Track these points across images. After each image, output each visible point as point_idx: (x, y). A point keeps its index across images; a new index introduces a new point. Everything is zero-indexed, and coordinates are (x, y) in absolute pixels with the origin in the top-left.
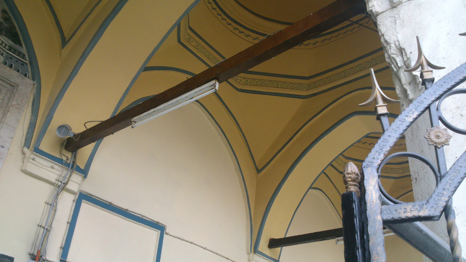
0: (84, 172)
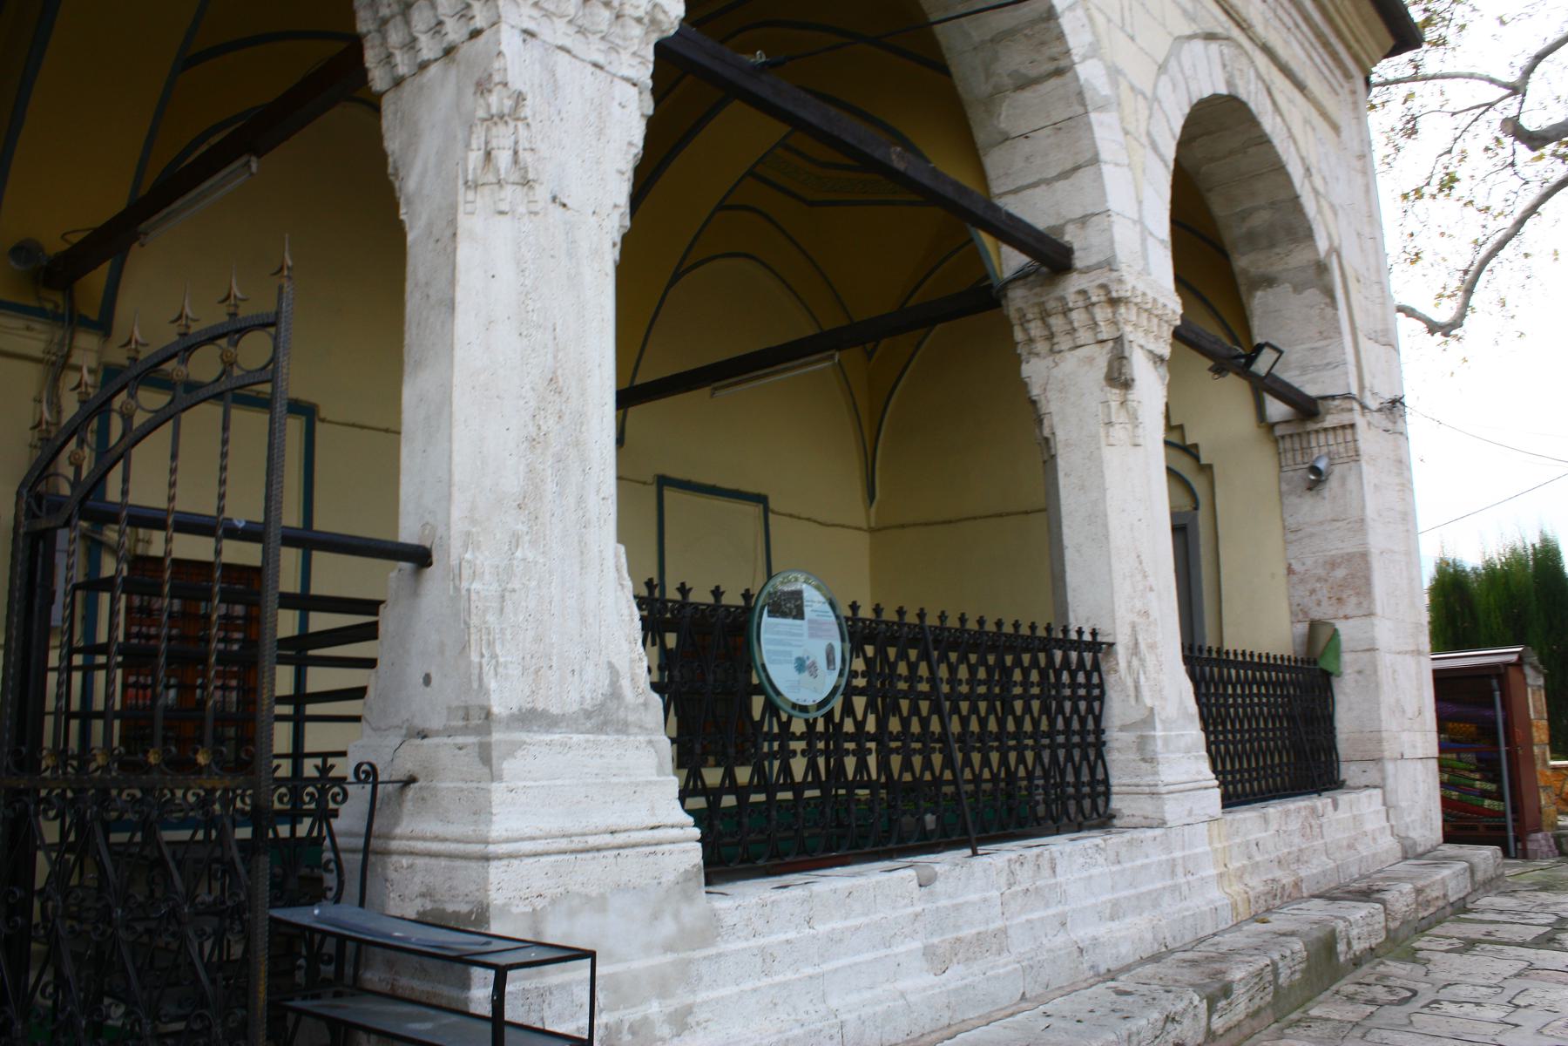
0: (104, 325)
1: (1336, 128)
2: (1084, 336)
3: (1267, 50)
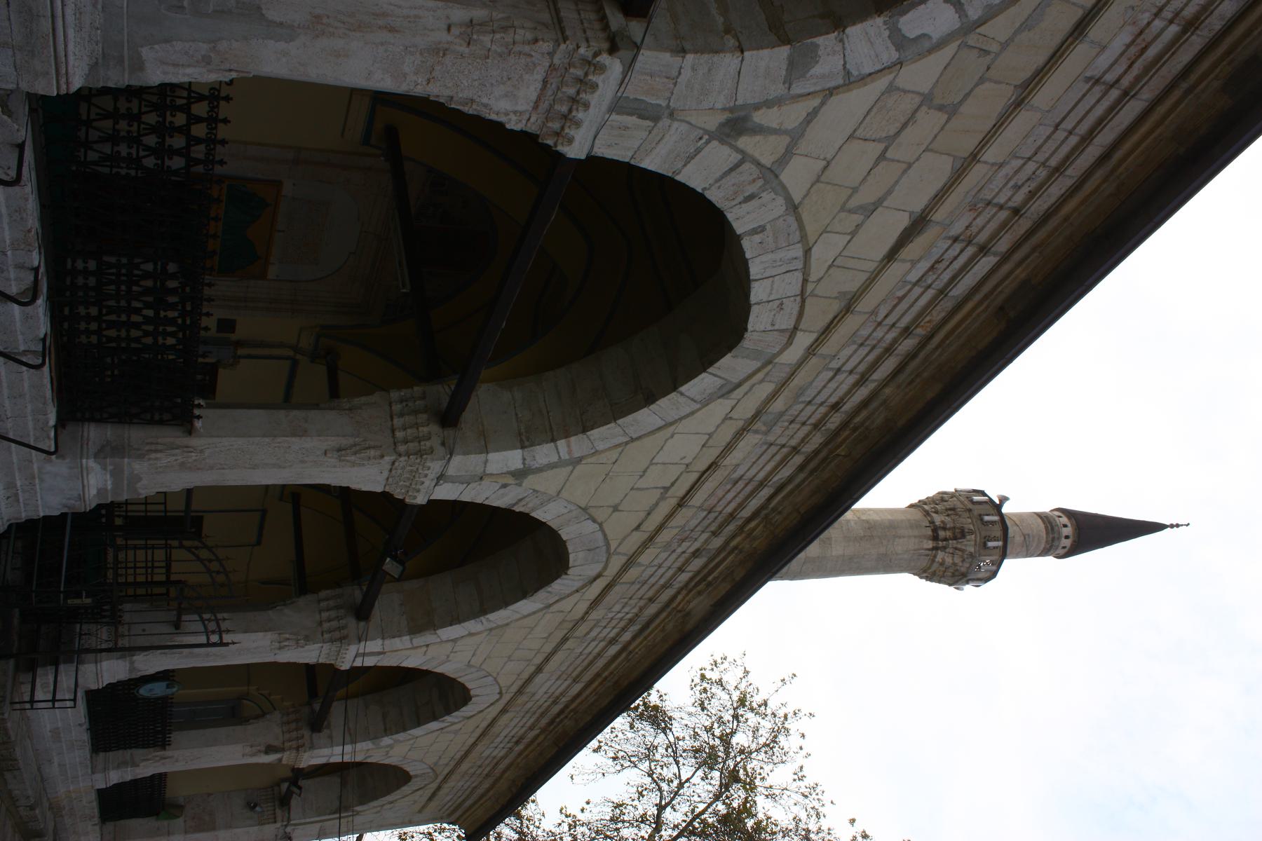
1: (420, 812)
2: (287, 736)
3: (439, 788)
